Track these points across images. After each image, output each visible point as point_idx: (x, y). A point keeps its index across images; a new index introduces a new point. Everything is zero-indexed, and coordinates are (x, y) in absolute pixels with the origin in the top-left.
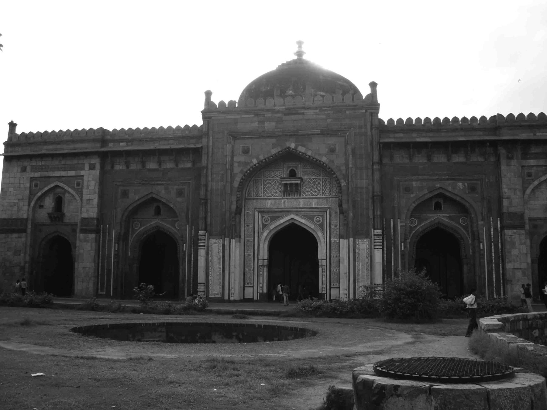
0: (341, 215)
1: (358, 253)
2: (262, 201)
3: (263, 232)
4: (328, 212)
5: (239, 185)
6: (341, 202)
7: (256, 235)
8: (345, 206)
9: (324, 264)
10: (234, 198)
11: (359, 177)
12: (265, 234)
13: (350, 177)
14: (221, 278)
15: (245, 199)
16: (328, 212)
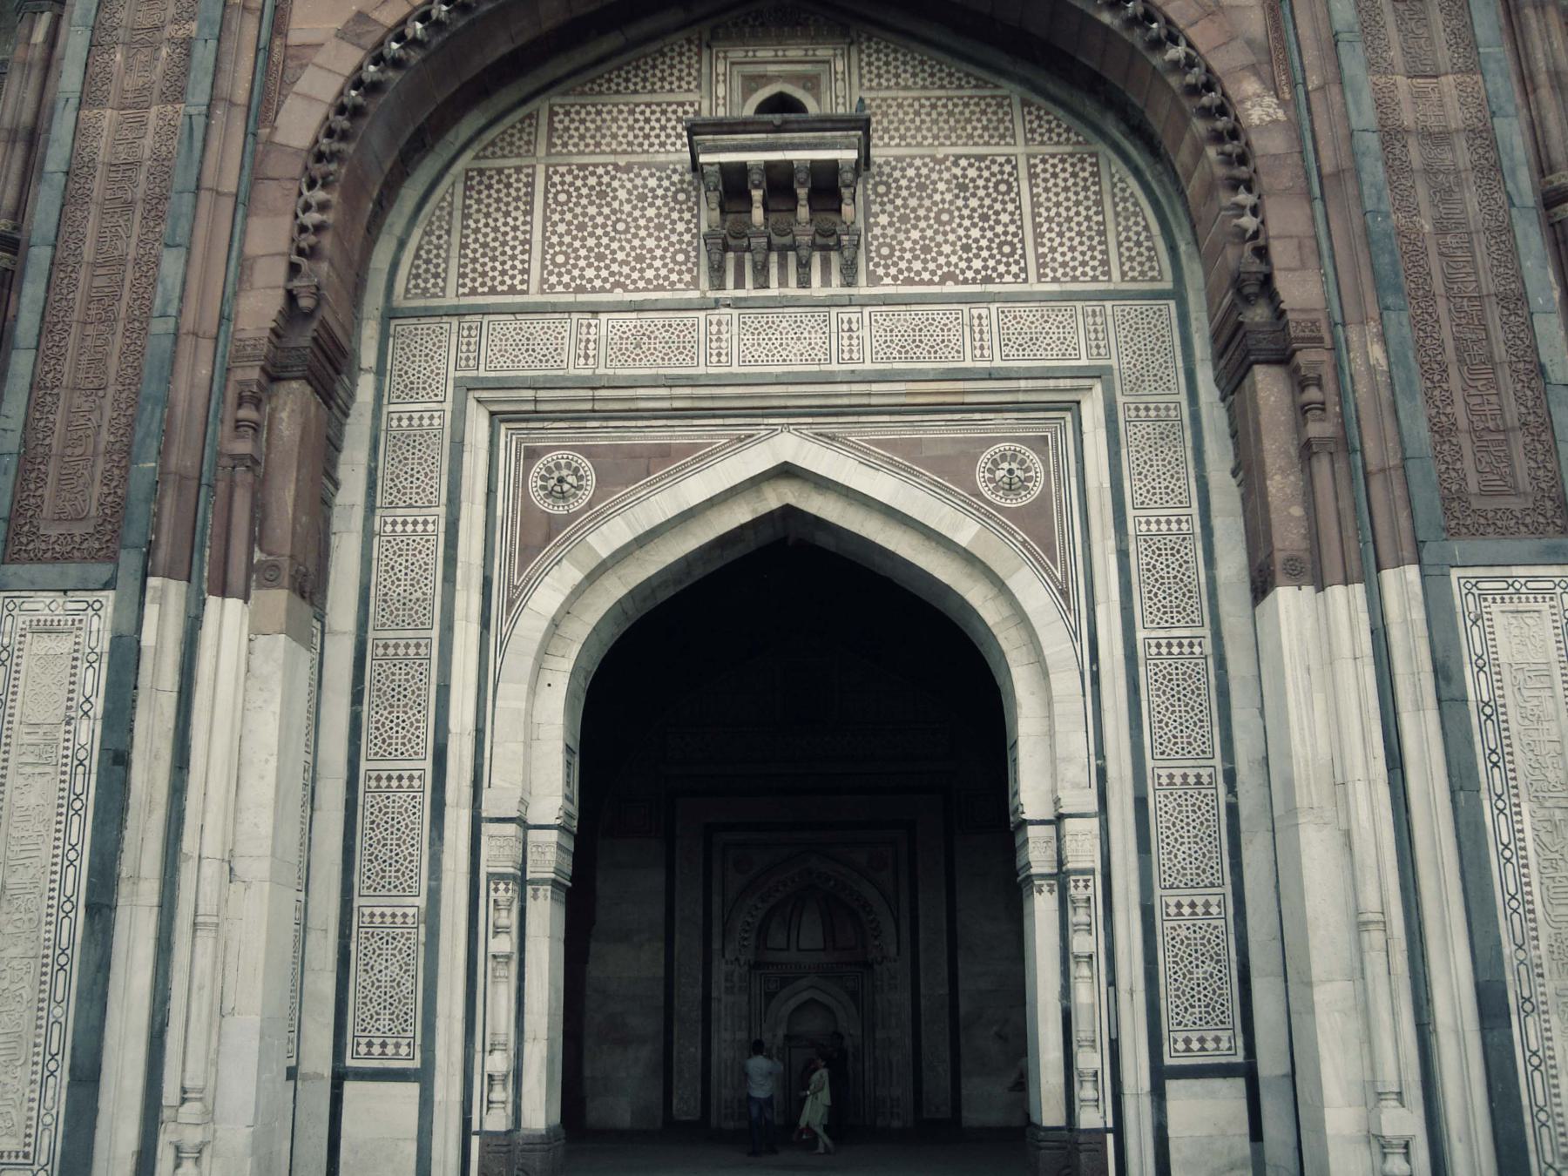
0: (1268, 385)
1: (1493, 710)
2: (536, 325)
3: (531, 584)
4: (1092, 411)
5: (330, 133)
6: (1262, 253)
7: (468, 602)
8: (1299, 290)
9: (1082, 848)
10: (270, 237)
11: (1395, 53)
12: (547, 597)
13: (1311, 56)
14: (68, 986)
15: (390, 314)
16: (1092, 411)
